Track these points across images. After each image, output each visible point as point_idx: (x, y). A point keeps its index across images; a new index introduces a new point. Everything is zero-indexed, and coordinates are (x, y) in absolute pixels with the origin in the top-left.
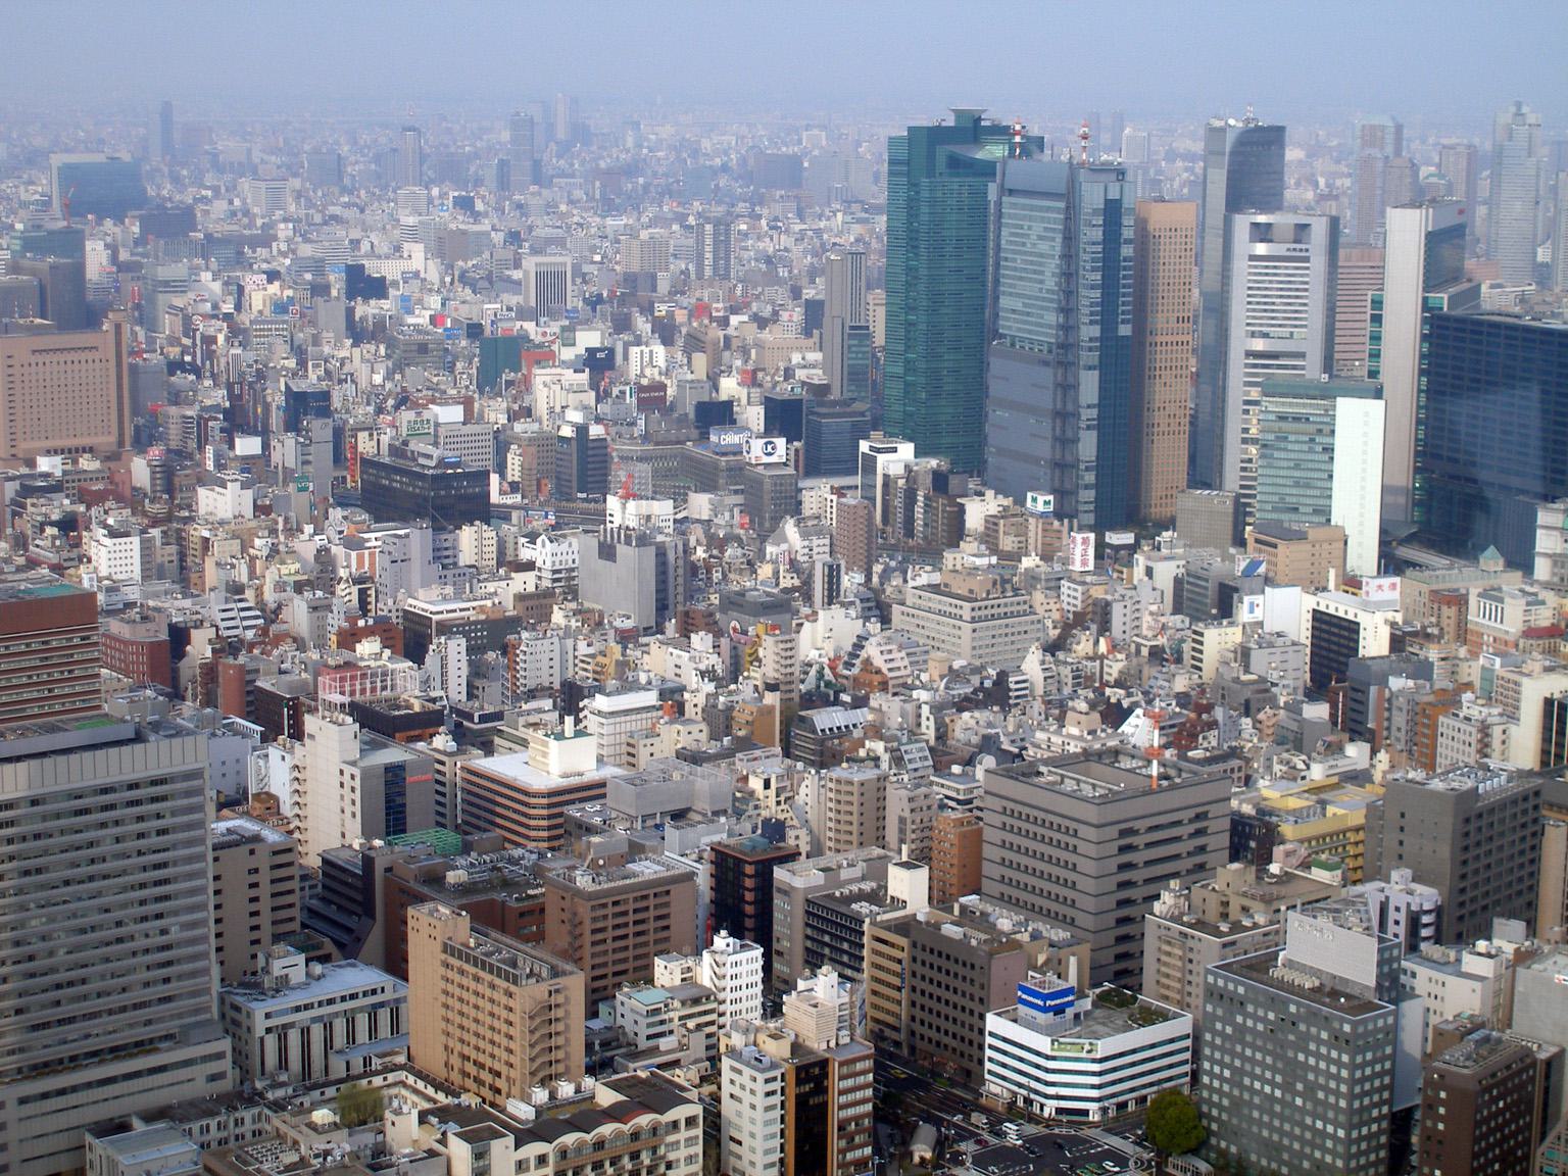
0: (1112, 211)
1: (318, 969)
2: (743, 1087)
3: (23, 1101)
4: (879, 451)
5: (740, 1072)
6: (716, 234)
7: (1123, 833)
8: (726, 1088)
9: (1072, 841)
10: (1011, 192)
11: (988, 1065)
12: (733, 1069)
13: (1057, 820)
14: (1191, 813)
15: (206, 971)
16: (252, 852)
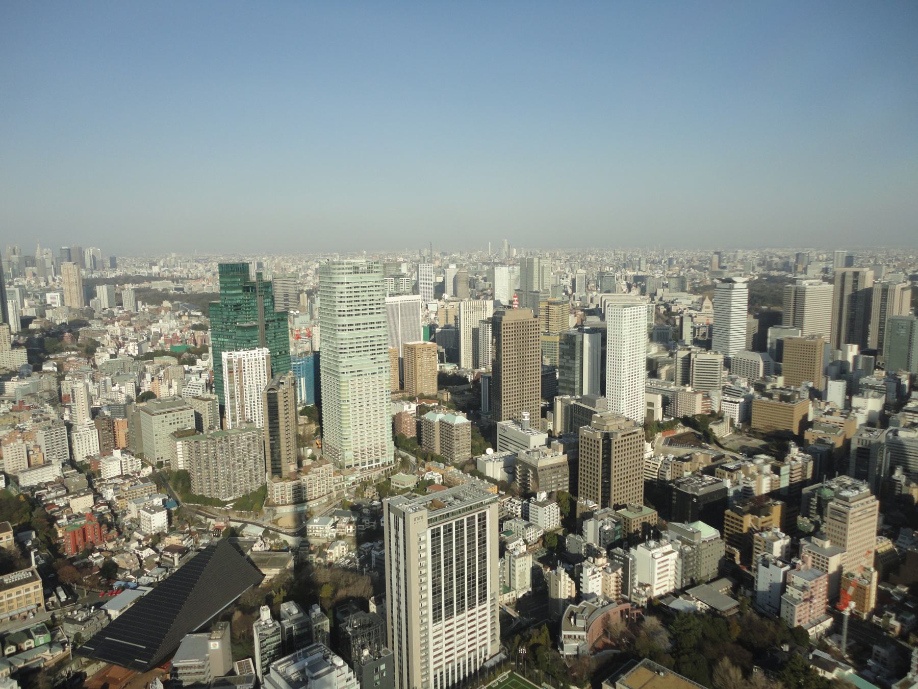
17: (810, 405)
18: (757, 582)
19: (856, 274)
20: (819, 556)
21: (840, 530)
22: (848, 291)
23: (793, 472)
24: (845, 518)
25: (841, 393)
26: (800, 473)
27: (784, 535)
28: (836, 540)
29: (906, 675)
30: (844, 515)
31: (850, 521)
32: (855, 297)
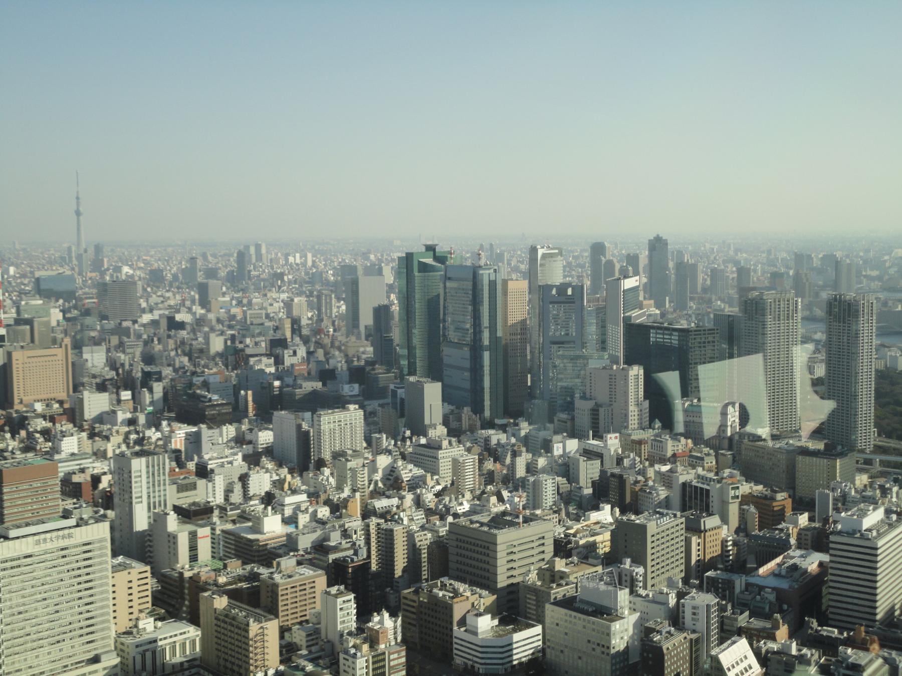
0: (493, 284)
1: (159, 624)
2: (349, 667)
4: (398, 388)
5: (348, 660)
6: (326, 300)
7: (508, 547)
8: (342, 667)
9: (487, 551)
10: (449, 279)
11: (455, 651)
12: (344, 659)
13: (480, 543)
14: (537, 537)
15: (109, 628)
16: (129, 573)
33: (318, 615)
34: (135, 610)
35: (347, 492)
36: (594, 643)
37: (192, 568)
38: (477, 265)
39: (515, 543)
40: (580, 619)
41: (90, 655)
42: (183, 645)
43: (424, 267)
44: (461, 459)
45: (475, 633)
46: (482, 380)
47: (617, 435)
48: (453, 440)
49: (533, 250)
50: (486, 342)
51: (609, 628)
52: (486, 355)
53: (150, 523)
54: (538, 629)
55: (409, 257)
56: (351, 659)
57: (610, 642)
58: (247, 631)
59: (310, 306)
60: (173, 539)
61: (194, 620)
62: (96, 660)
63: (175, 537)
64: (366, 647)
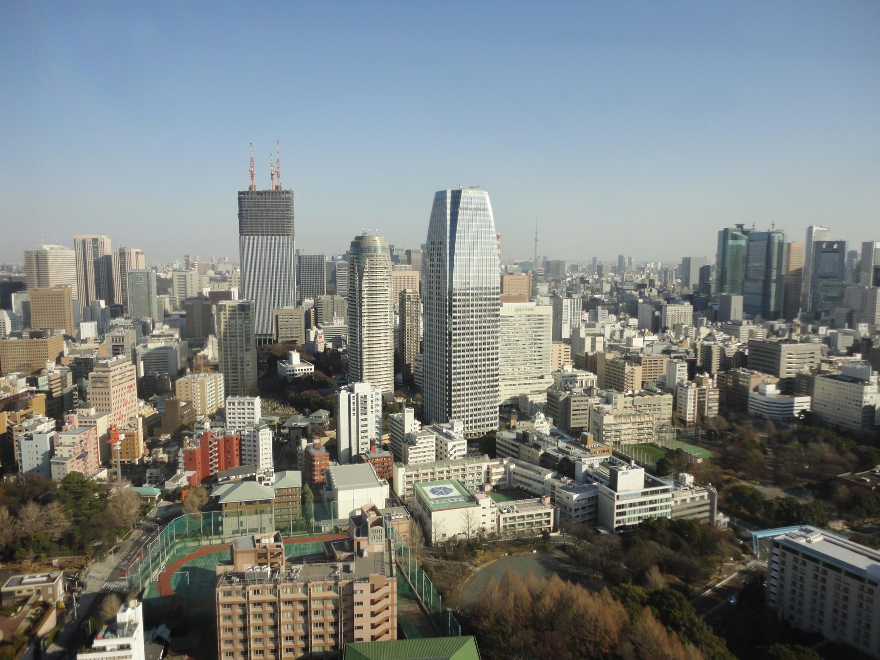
3: (506, 385)
8: (679, 395)
10: (752, 241)
17: (65, 345)
18: (21, 461)
19: (95, 241)
20: (86, 422)
21: (104, 396)
22: (90, 259)
23: (52, 383)
24: (107, 382)
25: (93, 331)
26: (60, 384)
27: (47, 418)
28: (101, 407)
29: (175, 473)
30: (105, 380)
31: (112, 384)
32: (97, 263)
33: (664, 377)
34: (562, 359)
35: (681, 338)
36: (850, 399)
37: (592, 351)
38: (771, 231)
39: (793, 352)
40: (840, 384)
41: (539, 375)
42: (587, 382)
43: (735, 237)
44: (755, 331)
45: (764, 394)
46: (769, 301)
47: (867, 324)
48: (750, 321)
49: (811, 228)
50: (774, 277)
51: (862, 389)
52: (773, 287)
53: (570, 335)
54: (808, 399)
55: (726, 231)
56: (684, 389)
57: (862, 398)
58: (624, 369)
59: (660, 280)
60: (583, 341)
61: (595, 373)
62: (542, 377)
63: (584, 340)
64: (694, 385)
